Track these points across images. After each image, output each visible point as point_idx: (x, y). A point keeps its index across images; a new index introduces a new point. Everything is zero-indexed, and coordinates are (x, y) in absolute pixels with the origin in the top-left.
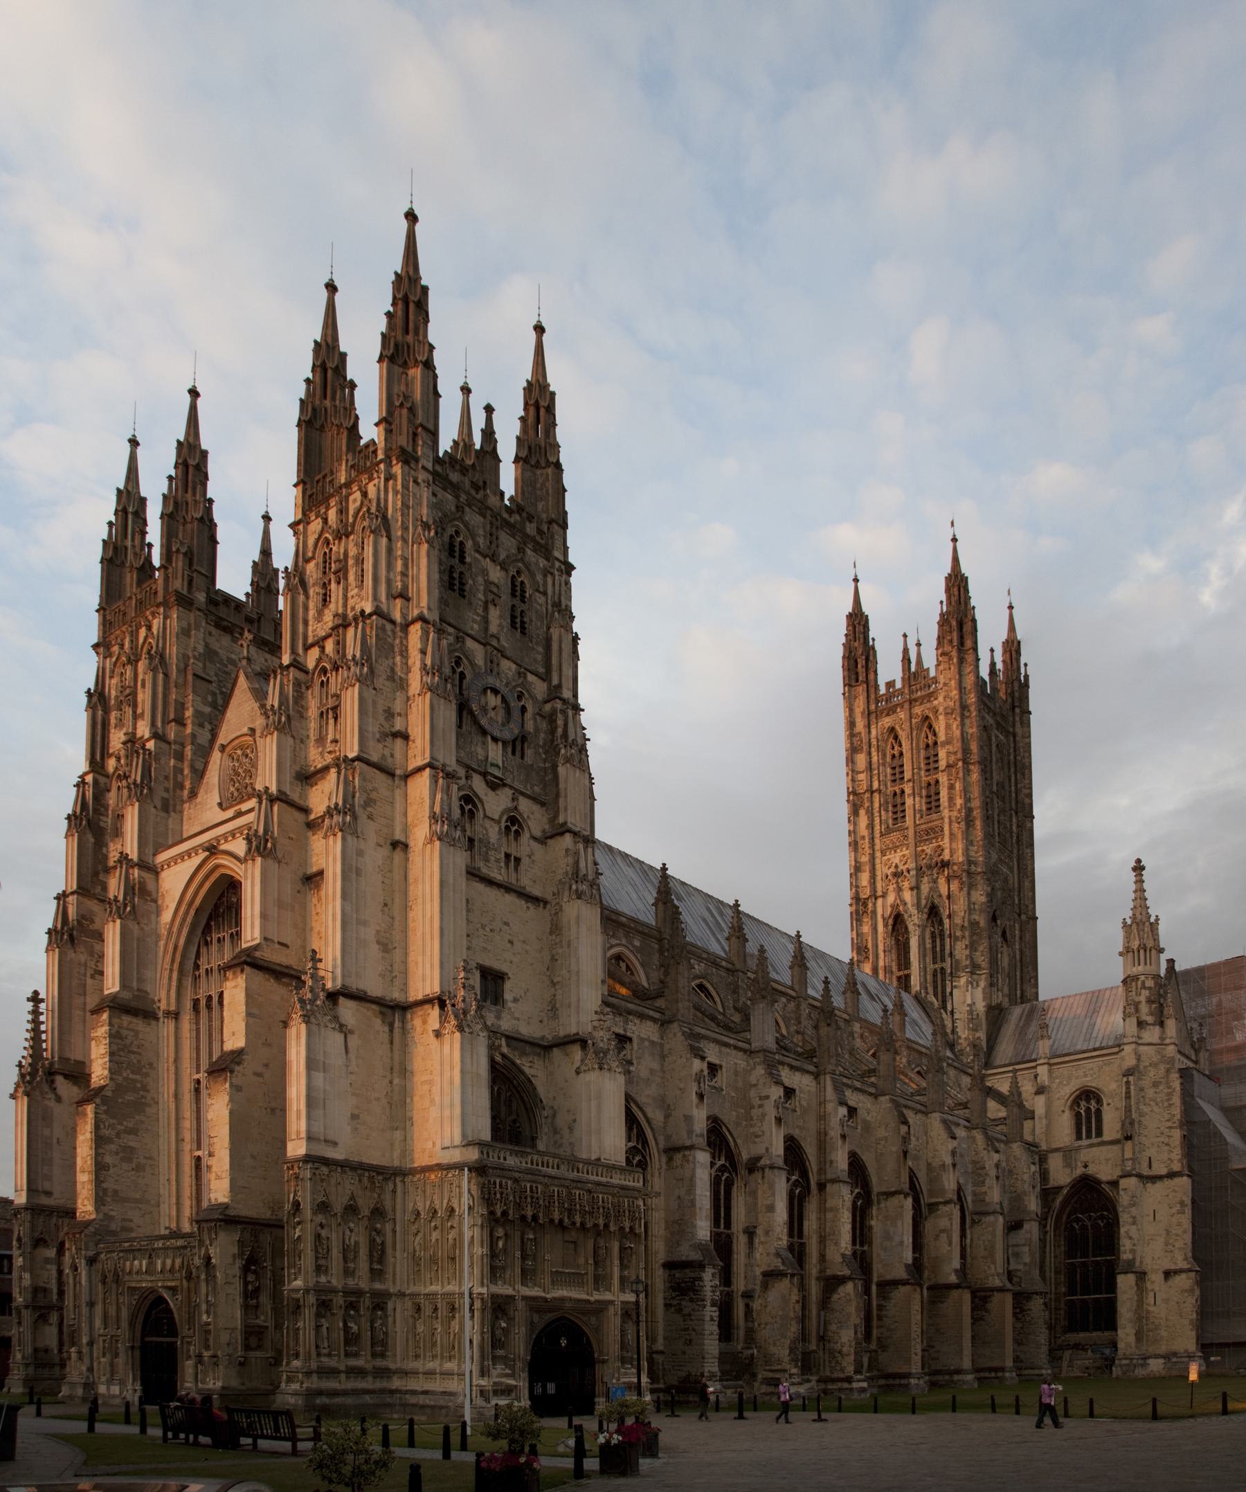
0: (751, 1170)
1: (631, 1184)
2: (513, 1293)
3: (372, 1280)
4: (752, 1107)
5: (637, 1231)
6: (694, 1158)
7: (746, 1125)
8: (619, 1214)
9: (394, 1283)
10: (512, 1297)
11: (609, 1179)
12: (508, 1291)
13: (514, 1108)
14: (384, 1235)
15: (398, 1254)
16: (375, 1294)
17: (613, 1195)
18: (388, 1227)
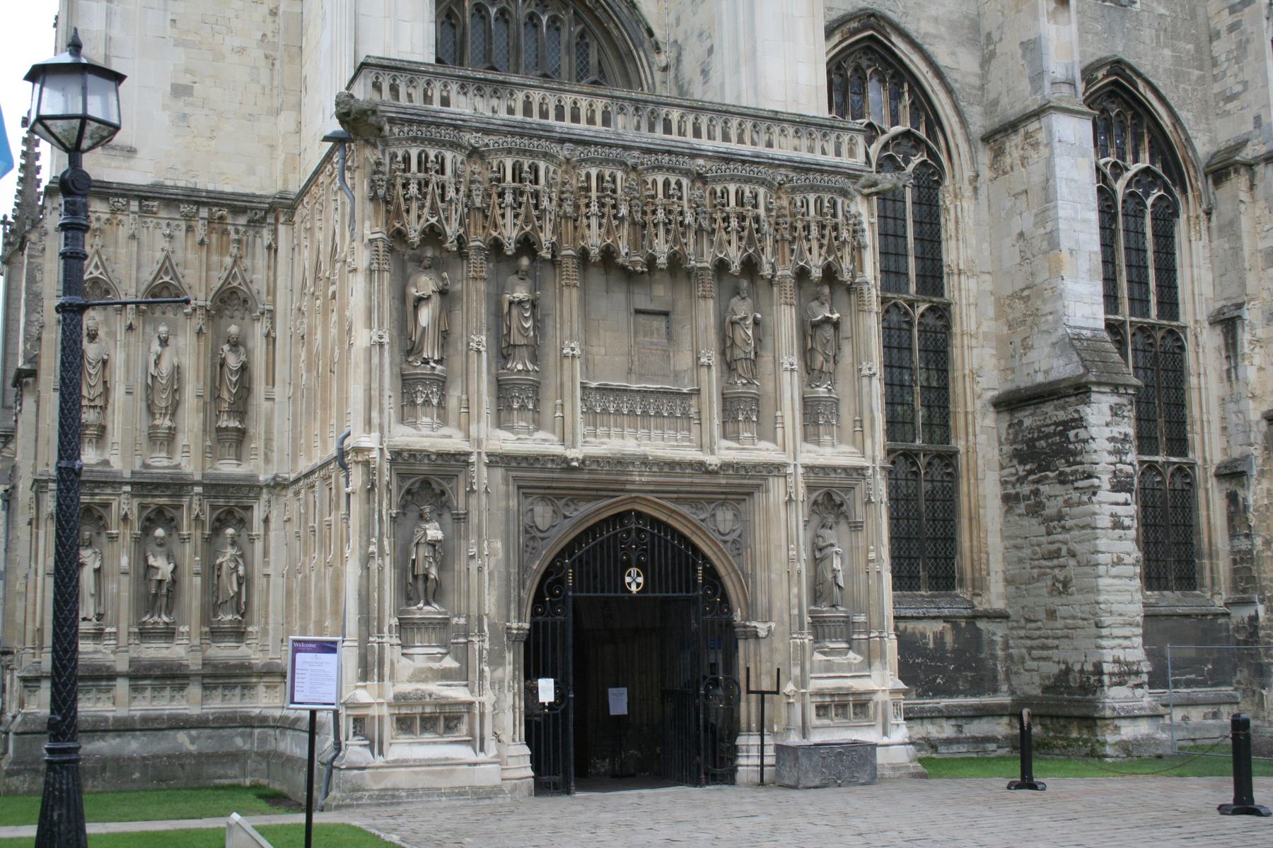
0: (1220, 171)
1: (831, 159)
2: (464, 447)
3: (212, 453)
4: (1214, 36)
5: (847, 277)
6: (1050, 132)
7: (1202, 78)
8: (789, 234)
9: (267, 460)
10: (460, 459)
11: (761, 149)
12: (451, 440)
13: (593, 59)
14: (248, 353)
15: (279, 392)
16: (215, 487)
17: (776, 188)
18: (259, 329)
